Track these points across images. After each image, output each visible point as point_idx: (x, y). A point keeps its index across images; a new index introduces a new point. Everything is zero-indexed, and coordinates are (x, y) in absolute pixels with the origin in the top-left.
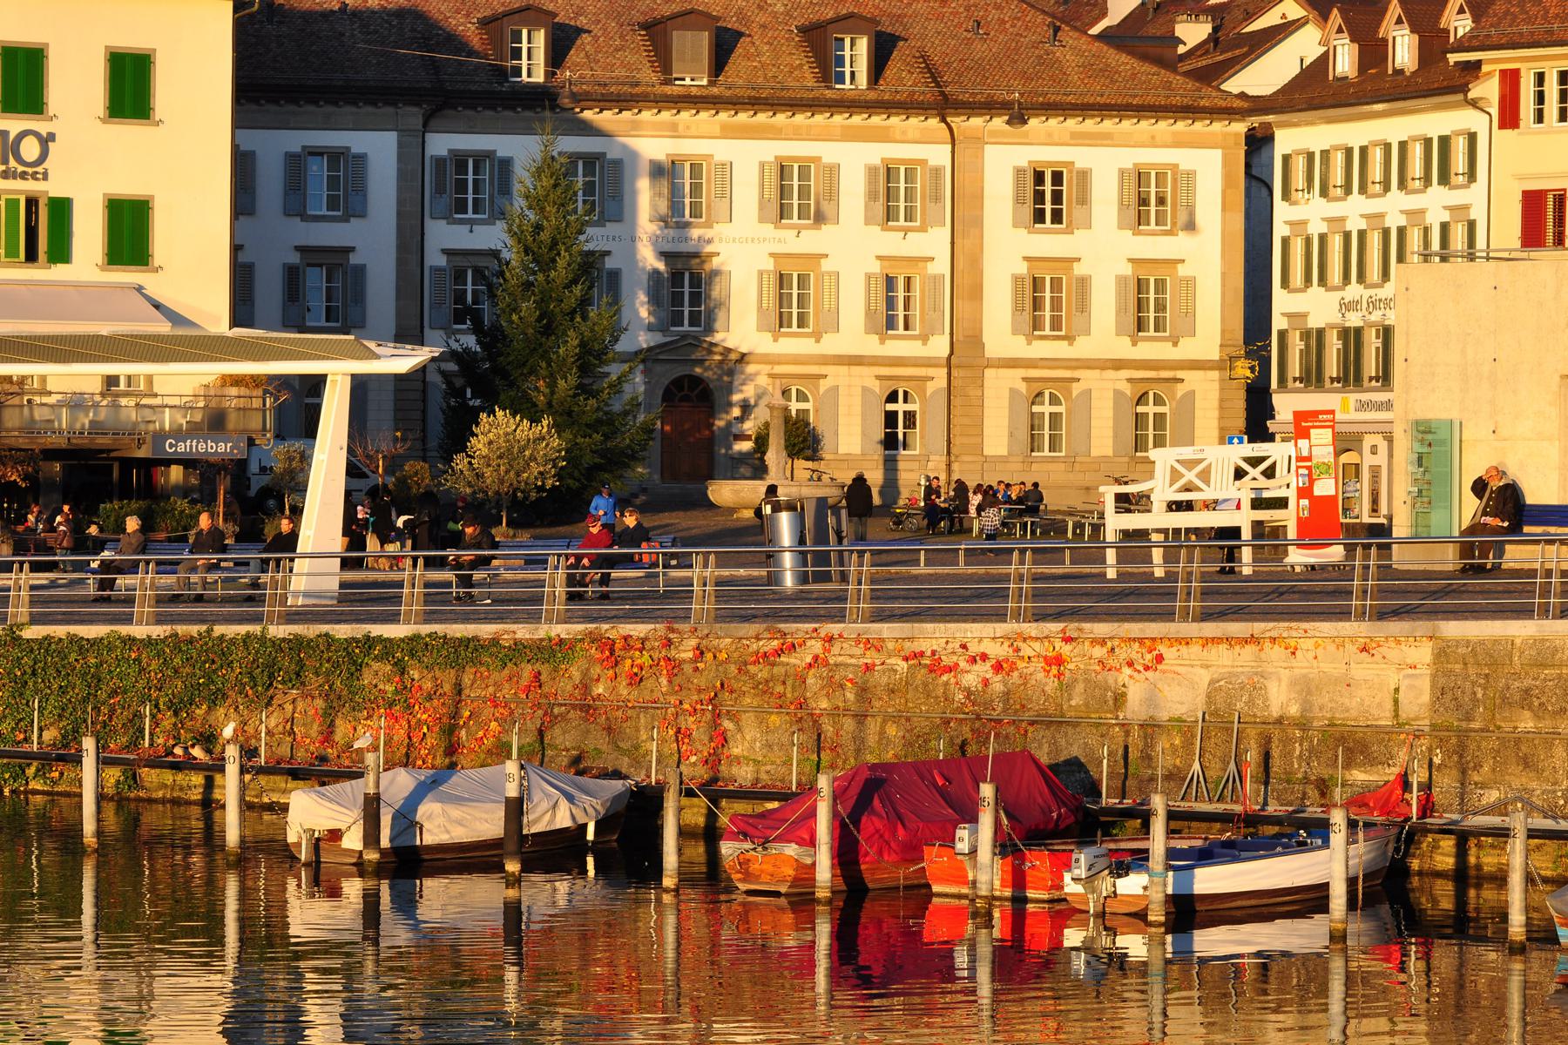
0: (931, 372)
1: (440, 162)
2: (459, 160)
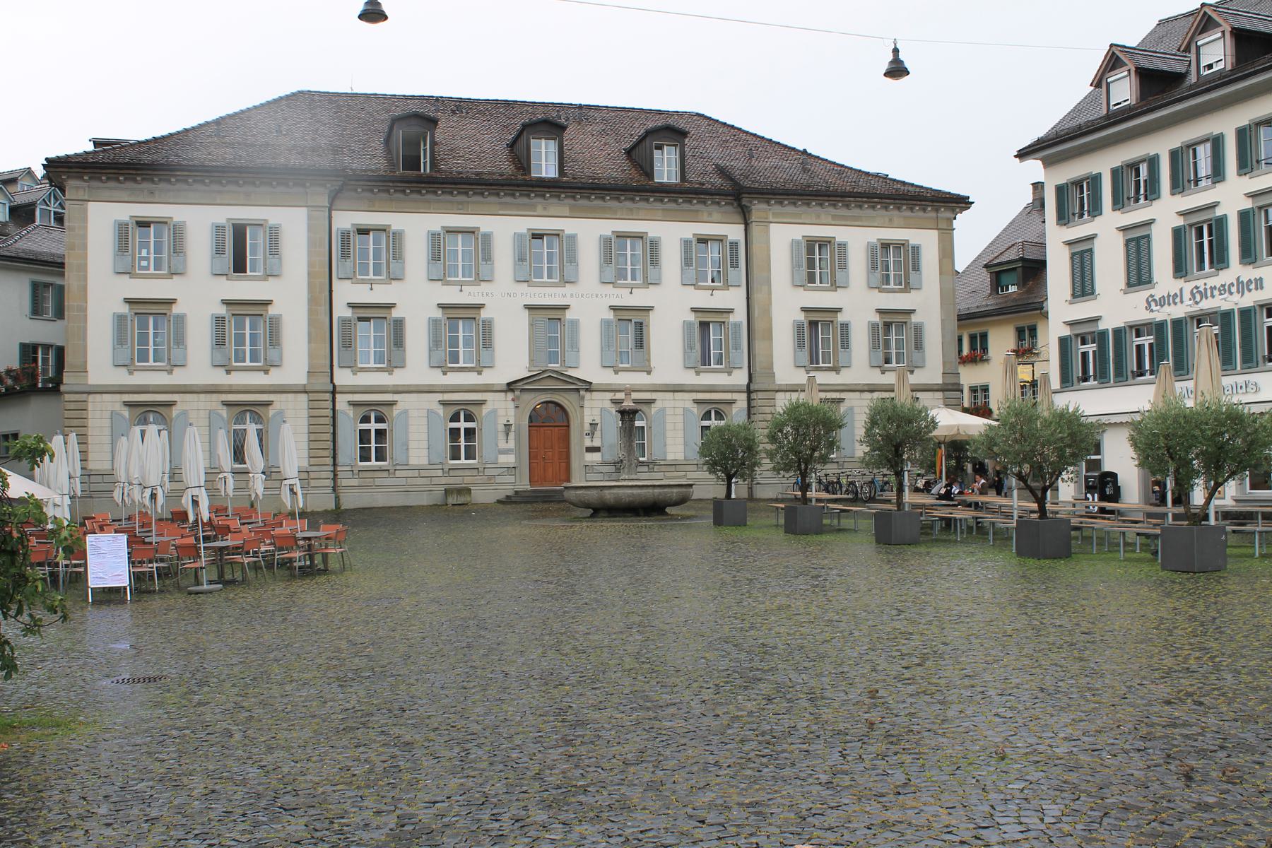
1: (345, 236)
2: (363, 231)
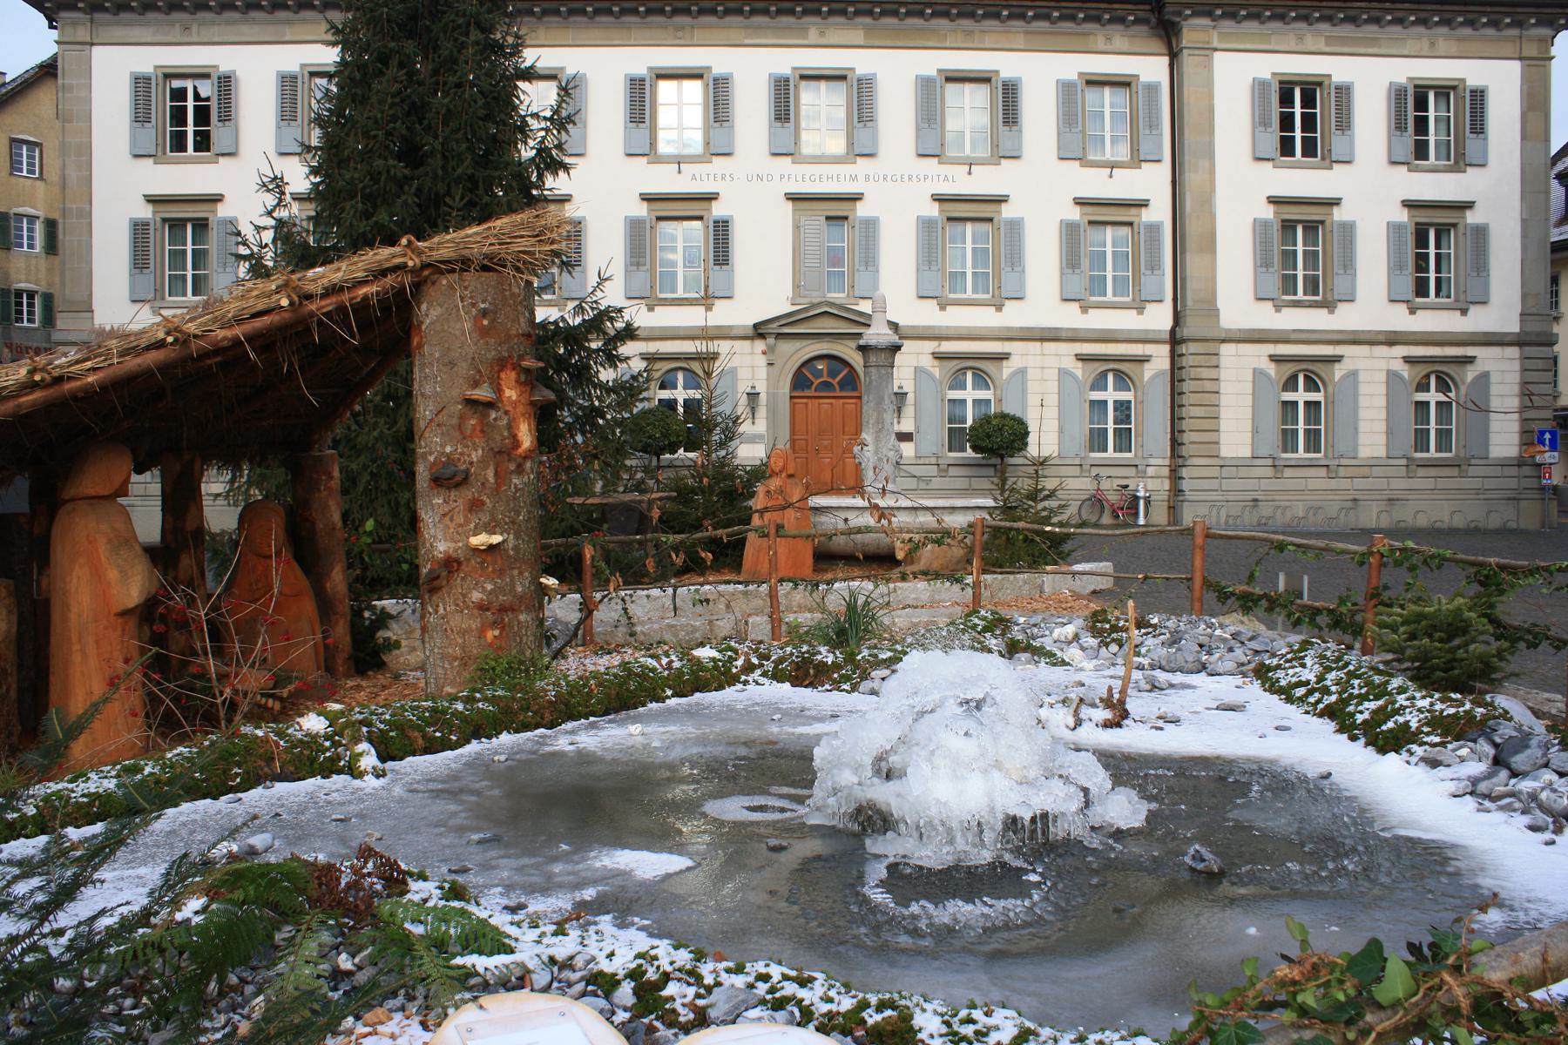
0: (1148, 349)
